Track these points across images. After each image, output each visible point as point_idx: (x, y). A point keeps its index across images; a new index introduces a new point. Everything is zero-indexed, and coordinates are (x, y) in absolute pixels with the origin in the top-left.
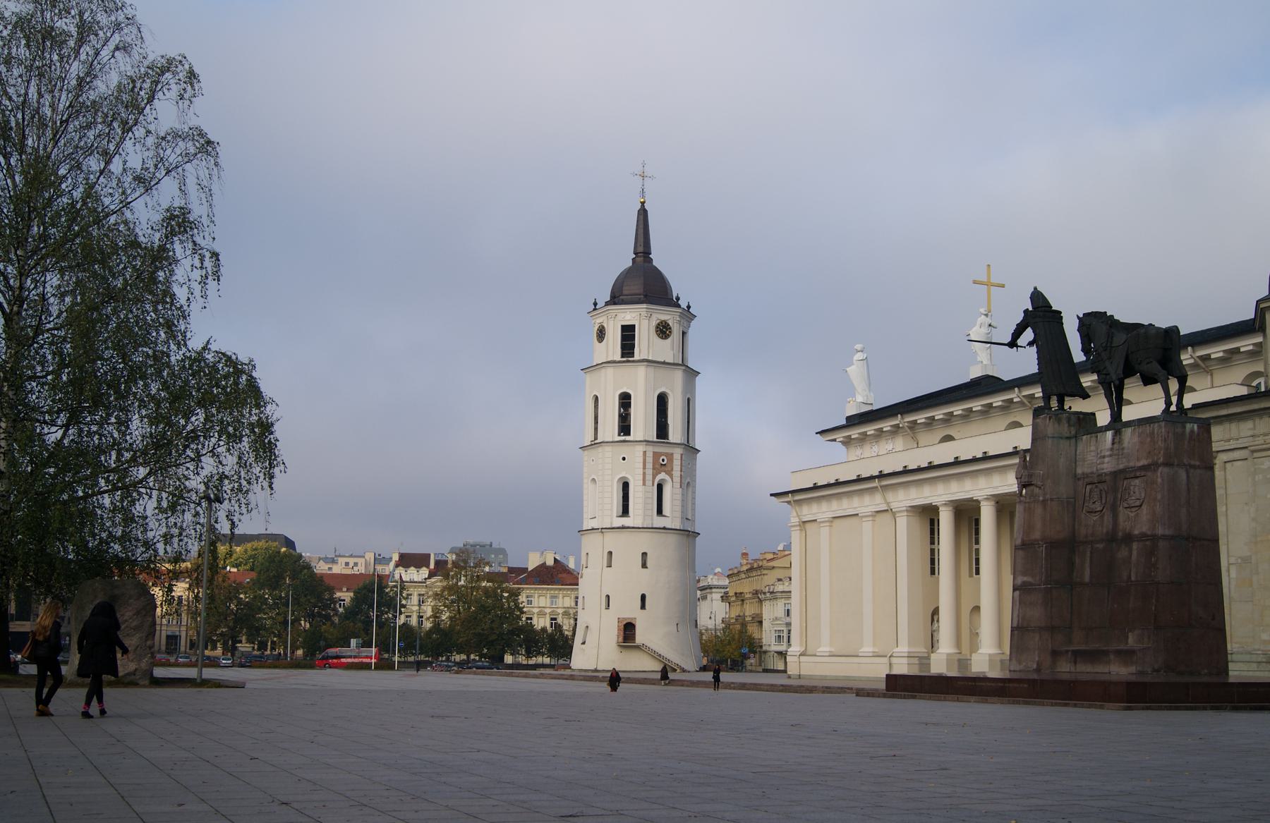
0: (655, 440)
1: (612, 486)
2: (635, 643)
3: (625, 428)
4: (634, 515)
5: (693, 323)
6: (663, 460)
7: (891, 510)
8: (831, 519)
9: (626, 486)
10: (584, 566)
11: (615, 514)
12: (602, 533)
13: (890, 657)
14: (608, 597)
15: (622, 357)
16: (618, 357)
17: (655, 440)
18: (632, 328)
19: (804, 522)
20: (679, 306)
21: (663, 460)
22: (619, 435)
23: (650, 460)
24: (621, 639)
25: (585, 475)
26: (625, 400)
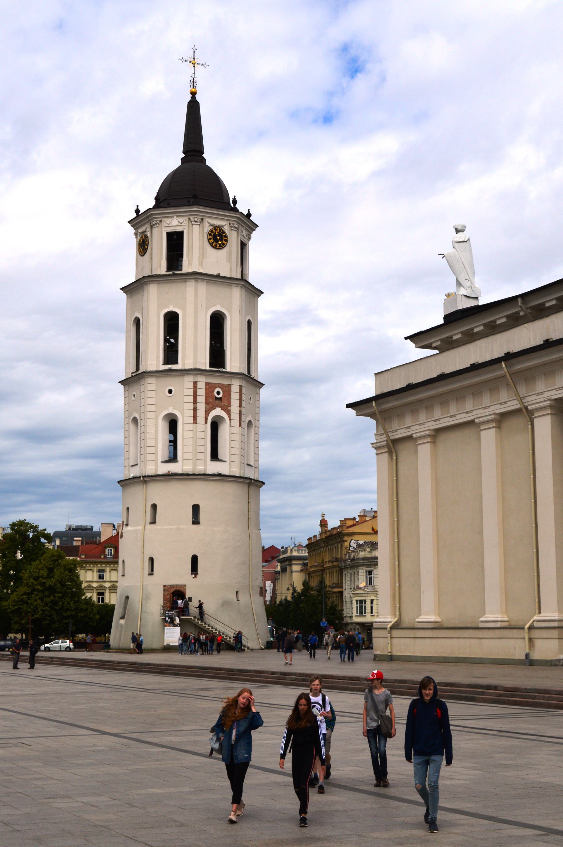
0: (208, 368)
1: (156, 425)
4: (183, 460)
5: (254, 234)
6: (218, 393)
7: (526, 408)
8: (432, 433)
10: (125, 523)
11: (160, 460)
13: (530, 628)
14: (151, 560)
15: (169, 269)
17: (208, 368)
18: (180, 235)
19: (395, 442)
20: (235, 210)
21: (218, 393)
23: (201, 392)
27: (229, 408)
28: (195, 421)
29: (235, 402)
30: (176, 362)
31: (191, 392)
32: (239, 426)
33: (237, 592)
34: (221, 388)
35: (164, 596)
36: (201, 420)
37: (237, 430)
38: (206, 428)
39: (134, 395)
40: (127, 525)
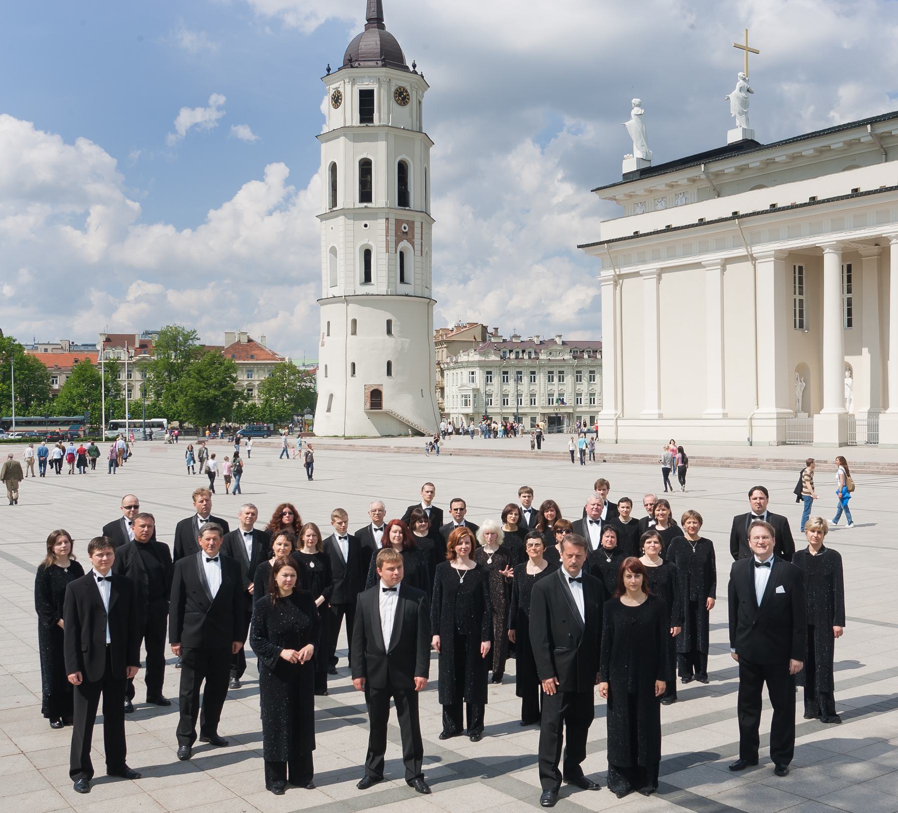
2: (381, 409)
3: (366, 195)
6: (405, 228)
7: (752, 255)
9: (367, 254)
11: (358, 281)
14: (353, 365)
15: (362, 121)
16: (356, 121)
18: (371, 92)
21: (405, 228)
23: (392, 227)
24: (368, 405)
25: (323, 244)
26: (366, 167)
27: (413, 240)
28: (387, 251)
29: (417, 236)
37: (419, 259)
38: (396, 256)
39: (332, 228)
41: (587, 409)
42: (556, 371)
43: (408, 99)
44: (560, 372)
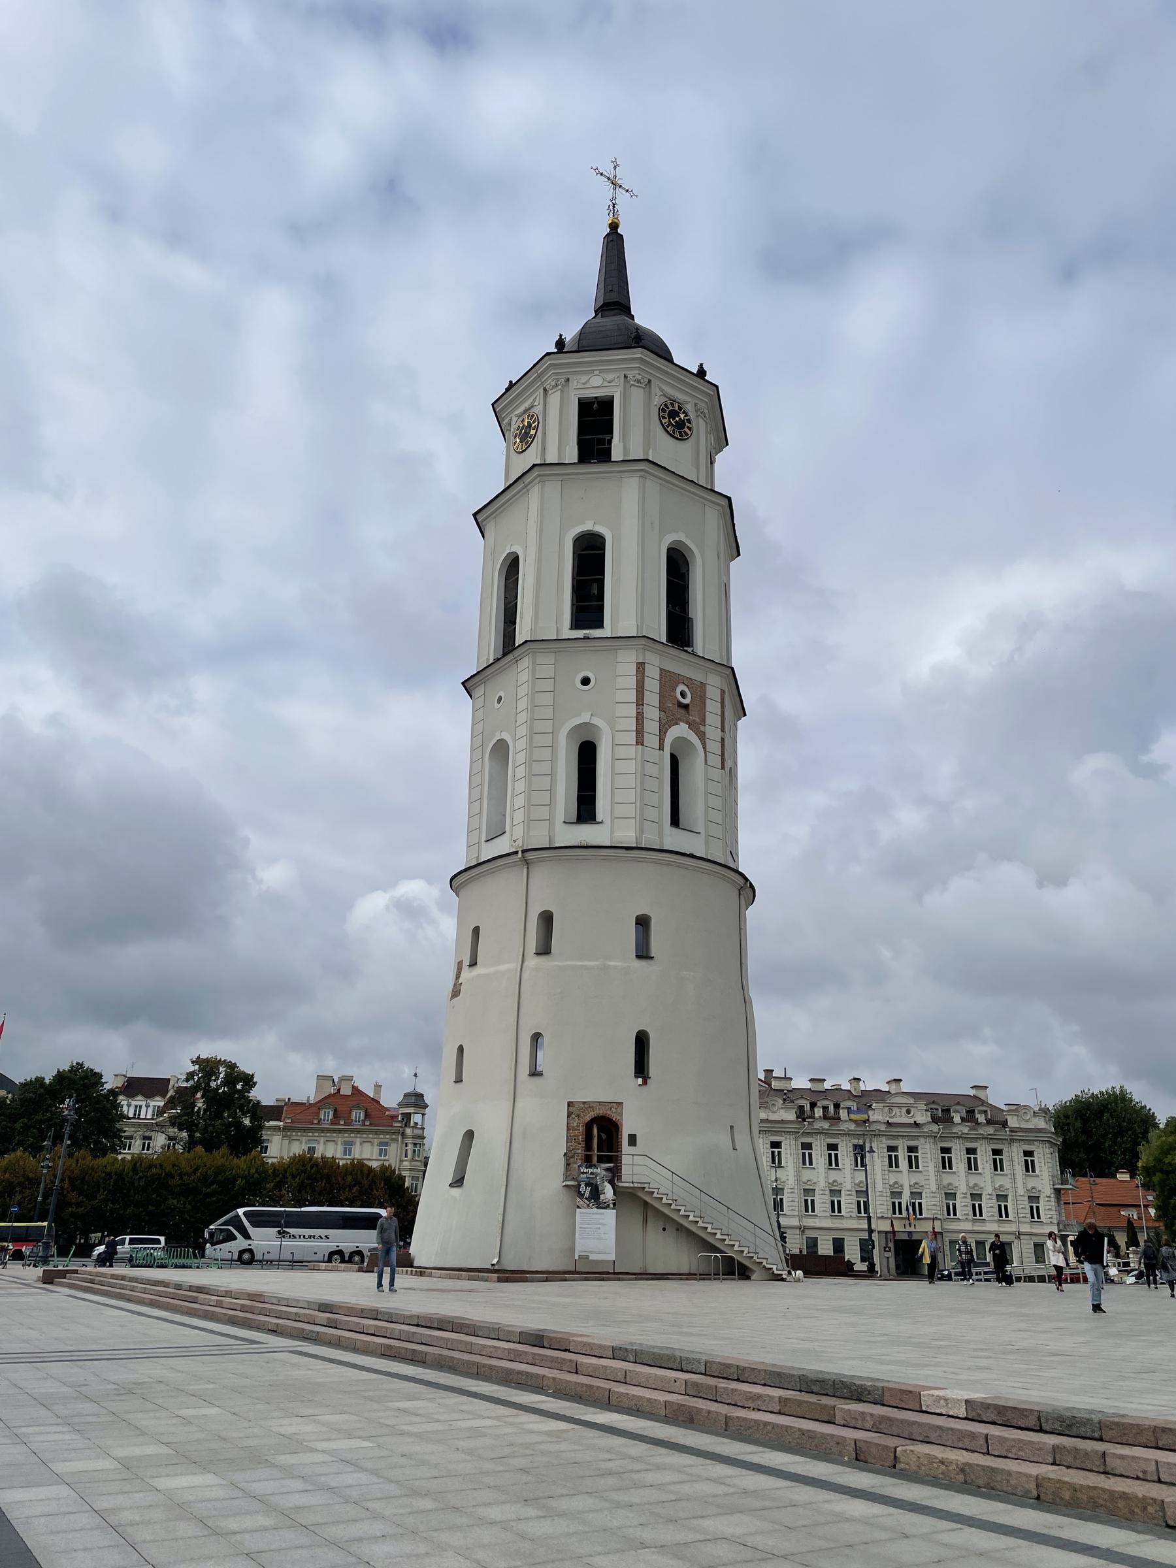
4: (613, 818)
6: (683, 695)
9: (587, 754)
11: (560, 816)
12: (527, 863)
18: (606, 405)
21: (683, 695)
22: (571, 628)
23: (653, 686)
27: (702, 728)
28: (640, 741)
29: (713, 719)
30: (600, 624)
31: (632, 682)
32: (722, 769)
33: (732, 1127)
34: (688, 686)
35: (568, 1129)
36: (652, 740)
38: (661, 758)
39: (500, 699)
40: (473, 964)
41: (968, 1226)
42: (902, 1145)
43: (690, 429)
44: (911, 1149)
